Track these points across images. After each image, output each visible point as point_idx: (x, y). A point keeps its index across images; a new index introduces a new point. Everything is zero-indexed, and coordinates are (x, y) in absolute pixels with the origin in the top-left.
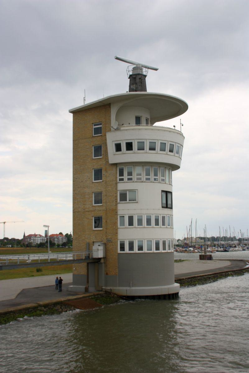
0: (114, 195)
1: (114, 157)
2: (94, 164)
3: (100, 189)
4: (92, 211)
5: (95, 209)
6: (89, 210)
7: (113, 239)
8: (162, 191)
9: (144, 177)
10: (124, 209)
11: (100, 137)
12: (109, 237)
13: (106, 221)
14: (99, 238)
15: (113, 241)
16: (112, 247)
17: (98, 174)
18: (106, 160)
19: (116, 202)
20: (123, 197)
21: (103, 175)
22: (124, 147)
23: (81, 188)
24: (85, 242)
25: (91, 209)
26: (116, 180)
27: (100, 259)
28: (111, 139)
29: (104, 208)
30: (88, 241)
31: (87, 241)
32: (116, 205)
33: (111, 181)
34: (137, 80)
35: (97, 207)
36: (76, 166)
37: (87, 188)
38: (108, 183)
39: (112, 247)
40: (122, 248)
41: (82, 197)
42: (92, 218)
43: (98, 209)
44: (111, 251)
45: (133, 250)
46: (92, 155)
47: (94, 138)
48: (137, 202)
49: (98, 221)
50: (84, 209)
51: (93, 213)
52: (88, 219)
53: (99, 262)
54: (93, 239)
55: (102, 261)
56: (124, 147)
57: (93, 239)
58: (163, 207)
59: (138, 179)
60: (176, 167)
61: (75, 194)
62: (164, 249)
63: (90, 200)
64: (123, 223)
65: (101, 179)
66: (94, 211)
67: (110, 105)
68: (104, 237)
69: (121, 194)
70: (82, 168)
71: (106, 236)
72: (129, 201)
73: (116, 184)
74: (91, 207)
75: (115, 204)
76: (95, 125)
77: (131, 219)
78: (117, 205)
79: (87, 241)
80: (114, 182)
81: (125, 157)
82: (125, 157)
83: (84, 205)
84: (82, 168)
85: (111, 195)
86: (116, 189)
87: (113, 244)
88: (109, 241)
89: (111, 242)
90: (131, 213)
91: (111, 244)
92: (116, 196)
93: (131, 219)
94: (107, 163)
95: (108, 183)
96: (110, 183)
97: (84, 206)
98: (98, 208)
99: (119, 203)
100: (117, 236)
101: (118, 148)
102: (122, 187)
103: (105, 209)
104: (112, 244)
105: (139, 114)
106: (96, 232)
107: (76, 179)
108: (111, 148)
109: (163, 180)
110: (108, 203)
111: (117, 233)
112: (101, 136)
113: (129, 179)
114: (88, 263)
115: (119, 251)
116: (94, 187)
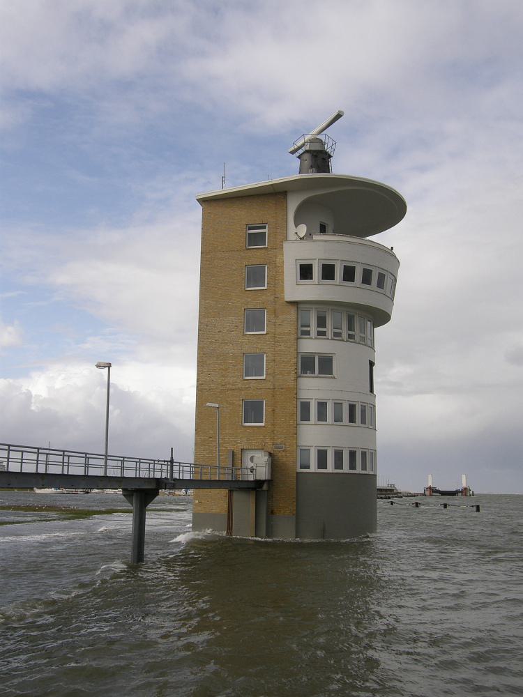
2: (249, 300)
4: (240, 389)
6: (234, 387)
9: (345, 332)
12: (279, 441)
17: (254, 320)
18: (275, 294)
22: (339, 273)
25: (240, 385)
27: (258, 484)
29: (269, 385)
30: (230, 447)
34: (319, 158)
36: (207, 301)
49: (253, 410)
51: (243, 392)
55: (265, 487)
56: (339, 273)
57: (243, 443)
59: (320, 333)
60: (382, 317)
64: (305, 416)
71: (273, 439)
77: (322, 406)
83: (223, 376)
90: (322, 396)
91: (284, 454)
93: (322, 406)
101: (306, 272)
108: (290, 272)
109: (363, 339)
113: (320, 333)
114: (231, 492)
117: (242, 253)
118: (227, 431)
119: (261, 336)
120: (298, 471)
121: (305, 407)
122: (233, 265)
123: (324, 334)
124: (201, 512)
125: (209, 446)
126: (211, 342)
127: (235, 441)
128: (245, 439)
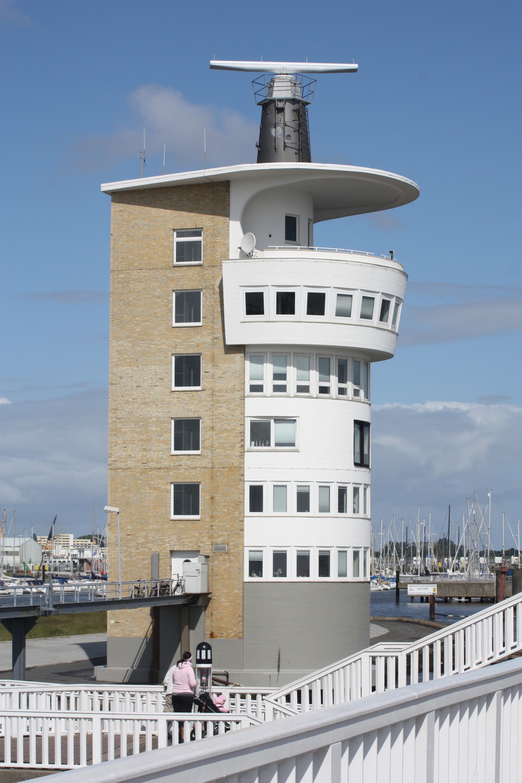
0: (235, 429)
1: (242, 328)
3: (194, 412)
4: (168, 468)
5: (177, 463)
6: (159, 466)
7: (231, 544)
8: (356, 422)
10: (260, 466)
11: (198, 268)
12: (220, 540)
13: (212, 498)
14: (191, 542)
15: (232, 551)
16: (228, 565)
18: (213, 333)
19: (243, 446)
20: (261, 433)
21: (202, 373)
23: (136, 405)
24: (147, 550)
25: (166, 463)
26: (243, 389)
28: (237, 278)
30: (155, 549)
31: (153, 549)
32: (242, 456)
33: (227, 392)
35: (187, 457)
36: (121, 342)
37: (154, 406)
38: (220, 396)
39: (228, 565)
40: (256, 567)
41: (138, 430)
42: (168, 488)
43: (188, 463)
44: (226, 576)
45: (284, 575)
46: (172, 316)
47: (177, 269)
48: (297, 451)
49: (187, 498)
50: (145, 461)
51: (171, 473)
52: (155, 489)
53: (194, 606)
54: (172, 543)
57: (172, 543)
58: (356, 464)
61: (117, 418)
62: (356, 573)
63: (162, 438)
64: (257, 504)
65: (198, 384)
66: (176, 468)
67: (229, 186)
68: (205, 539)
69: (253, 425)
70: (138, 349)
71: (211, 537)
72: (277, 445)
73: (243, 398)
74: (165, 456)
75: (238, 454)
76: (179, 235)
78: (243, 455)
79: (153, 549)
80: (238, 395)
81: (272, 329)
82: (272, 329)
83: (145, 450)
84: (138, 349)
85: (228, 428)
86: (243, 413)
87: (232, 558)
88: (220, 550)
89: (226, 553)
90: (280, 477)
91: (226, 557)
92: (243, 433)
94: (215, 340)
95: (220, 396)
96: (223, 396)
97: (145, 453)
98: (188, 460)
99: (248, 451)
100: (242, 537)
101: (254, 304)
102: (256, 407)
103: (210, 466)
104: (229, 559)
105: (293, 212)
106: (181, 525)
107: (121, 377)
110: (218, 450)
111: (242, 530)
112: (200, 265)
113: (278, 389)
115: (247, 578)
116: (175, 405)
117: (168, 272)
118: (151, 527)
119: (195, 393)
120: (245, 581)
121: (257, 493)
122: (155, 290)
123: (282, 389)
124: (119, 636)
125: (127, 547)
126: (127, 402)
127: (162, 541)
128: (174, 538)
